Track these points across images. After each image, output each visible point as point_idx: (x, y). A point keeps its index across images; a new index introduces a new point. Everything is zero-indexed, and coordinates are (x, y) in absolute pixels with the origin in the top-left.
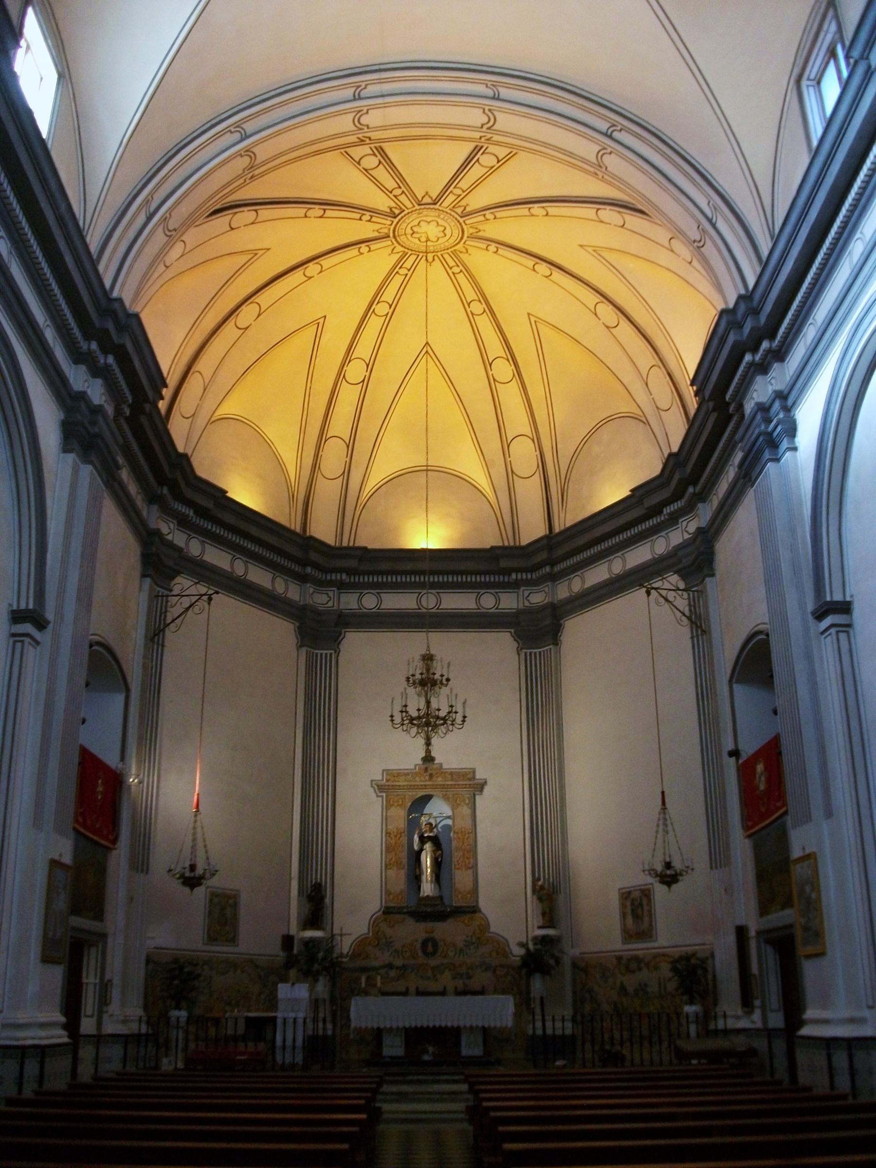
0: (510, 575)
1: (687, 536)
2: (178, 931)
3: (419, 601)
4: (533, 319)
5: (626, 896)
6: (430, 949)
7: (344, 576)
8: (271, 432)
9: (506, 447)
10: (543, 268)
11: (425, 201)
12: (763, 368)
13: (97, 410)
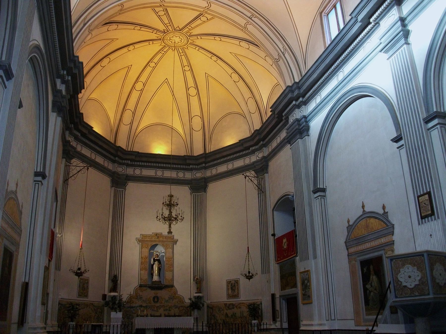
0: (189, 165)
1: (258, 158)
2: (69, 293)
3: (156, 173)
4: (207, 75)
5: (229, 282)
6: (156, 300)
7: (129, 162)
8: (106, 106)
10: (214, 58)
11: (177, 29)
12: (299, 106)
13: (63, 97)
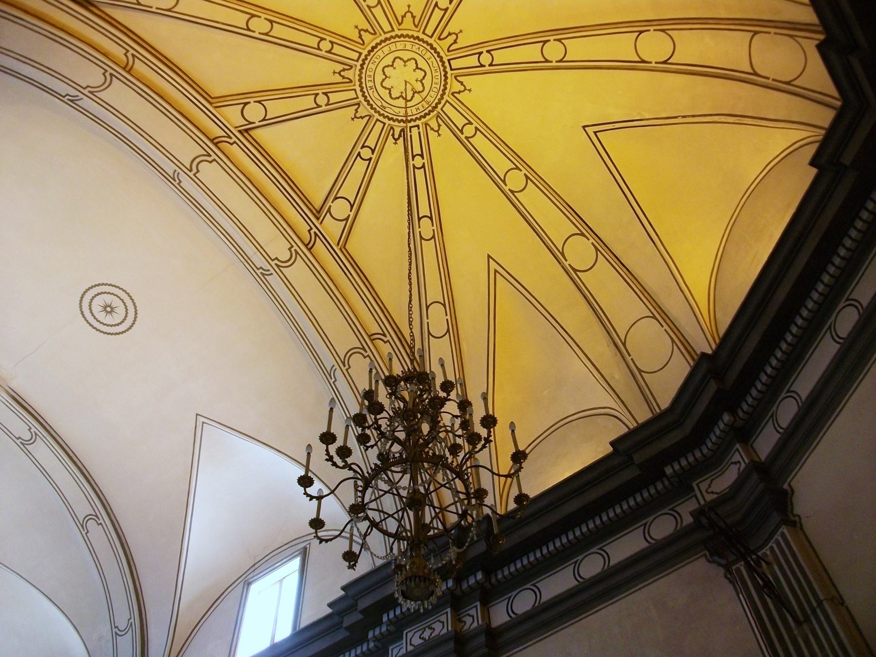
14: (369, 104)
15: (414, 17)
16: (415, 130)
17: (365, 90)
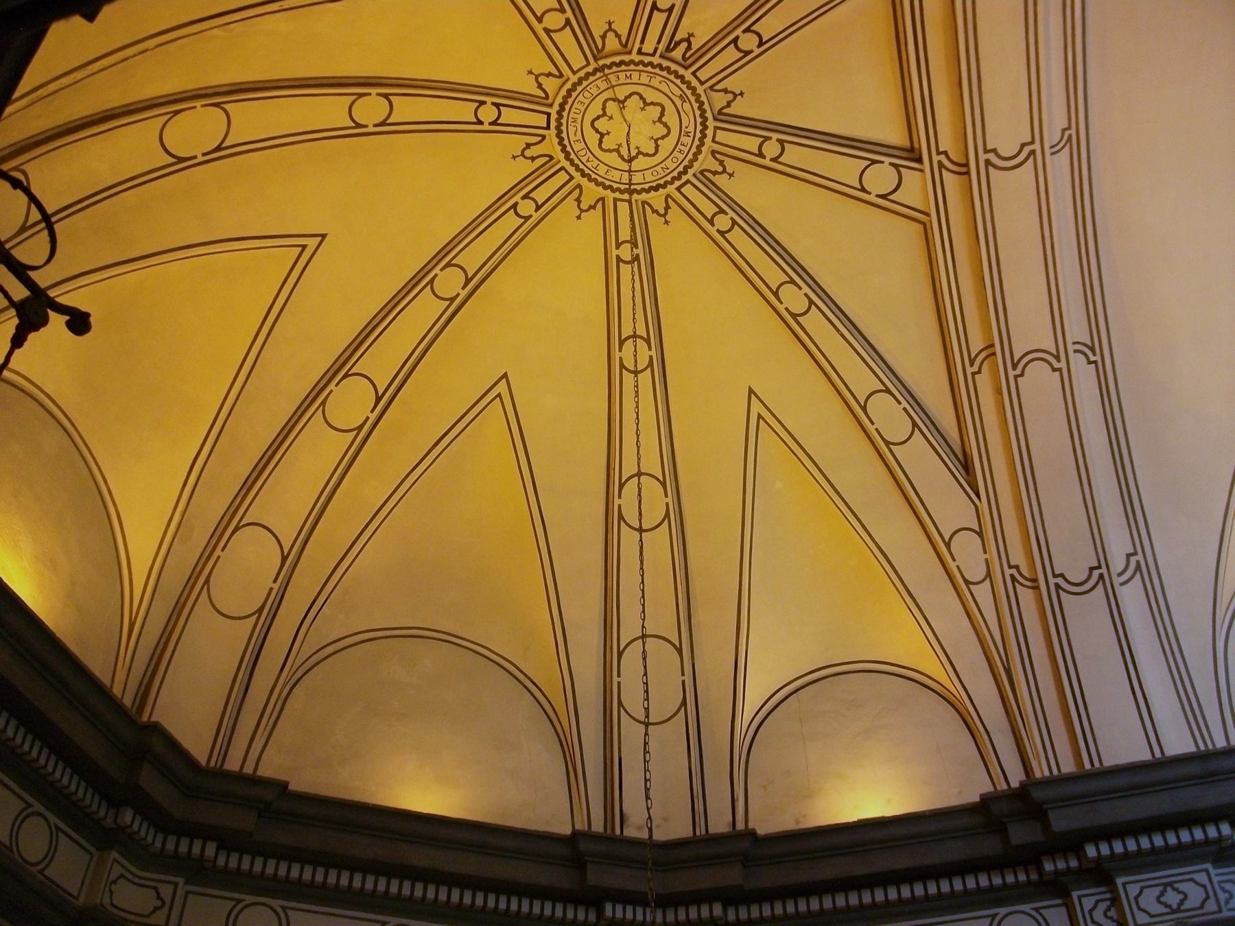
0: (116, 804)
9: (231, 522)
14: (703, 112)
15: (578, 200)
16: (648, 47)
17: (698, 135)
